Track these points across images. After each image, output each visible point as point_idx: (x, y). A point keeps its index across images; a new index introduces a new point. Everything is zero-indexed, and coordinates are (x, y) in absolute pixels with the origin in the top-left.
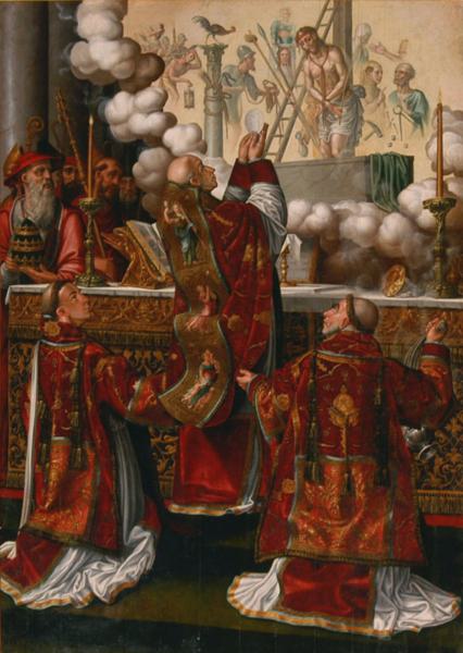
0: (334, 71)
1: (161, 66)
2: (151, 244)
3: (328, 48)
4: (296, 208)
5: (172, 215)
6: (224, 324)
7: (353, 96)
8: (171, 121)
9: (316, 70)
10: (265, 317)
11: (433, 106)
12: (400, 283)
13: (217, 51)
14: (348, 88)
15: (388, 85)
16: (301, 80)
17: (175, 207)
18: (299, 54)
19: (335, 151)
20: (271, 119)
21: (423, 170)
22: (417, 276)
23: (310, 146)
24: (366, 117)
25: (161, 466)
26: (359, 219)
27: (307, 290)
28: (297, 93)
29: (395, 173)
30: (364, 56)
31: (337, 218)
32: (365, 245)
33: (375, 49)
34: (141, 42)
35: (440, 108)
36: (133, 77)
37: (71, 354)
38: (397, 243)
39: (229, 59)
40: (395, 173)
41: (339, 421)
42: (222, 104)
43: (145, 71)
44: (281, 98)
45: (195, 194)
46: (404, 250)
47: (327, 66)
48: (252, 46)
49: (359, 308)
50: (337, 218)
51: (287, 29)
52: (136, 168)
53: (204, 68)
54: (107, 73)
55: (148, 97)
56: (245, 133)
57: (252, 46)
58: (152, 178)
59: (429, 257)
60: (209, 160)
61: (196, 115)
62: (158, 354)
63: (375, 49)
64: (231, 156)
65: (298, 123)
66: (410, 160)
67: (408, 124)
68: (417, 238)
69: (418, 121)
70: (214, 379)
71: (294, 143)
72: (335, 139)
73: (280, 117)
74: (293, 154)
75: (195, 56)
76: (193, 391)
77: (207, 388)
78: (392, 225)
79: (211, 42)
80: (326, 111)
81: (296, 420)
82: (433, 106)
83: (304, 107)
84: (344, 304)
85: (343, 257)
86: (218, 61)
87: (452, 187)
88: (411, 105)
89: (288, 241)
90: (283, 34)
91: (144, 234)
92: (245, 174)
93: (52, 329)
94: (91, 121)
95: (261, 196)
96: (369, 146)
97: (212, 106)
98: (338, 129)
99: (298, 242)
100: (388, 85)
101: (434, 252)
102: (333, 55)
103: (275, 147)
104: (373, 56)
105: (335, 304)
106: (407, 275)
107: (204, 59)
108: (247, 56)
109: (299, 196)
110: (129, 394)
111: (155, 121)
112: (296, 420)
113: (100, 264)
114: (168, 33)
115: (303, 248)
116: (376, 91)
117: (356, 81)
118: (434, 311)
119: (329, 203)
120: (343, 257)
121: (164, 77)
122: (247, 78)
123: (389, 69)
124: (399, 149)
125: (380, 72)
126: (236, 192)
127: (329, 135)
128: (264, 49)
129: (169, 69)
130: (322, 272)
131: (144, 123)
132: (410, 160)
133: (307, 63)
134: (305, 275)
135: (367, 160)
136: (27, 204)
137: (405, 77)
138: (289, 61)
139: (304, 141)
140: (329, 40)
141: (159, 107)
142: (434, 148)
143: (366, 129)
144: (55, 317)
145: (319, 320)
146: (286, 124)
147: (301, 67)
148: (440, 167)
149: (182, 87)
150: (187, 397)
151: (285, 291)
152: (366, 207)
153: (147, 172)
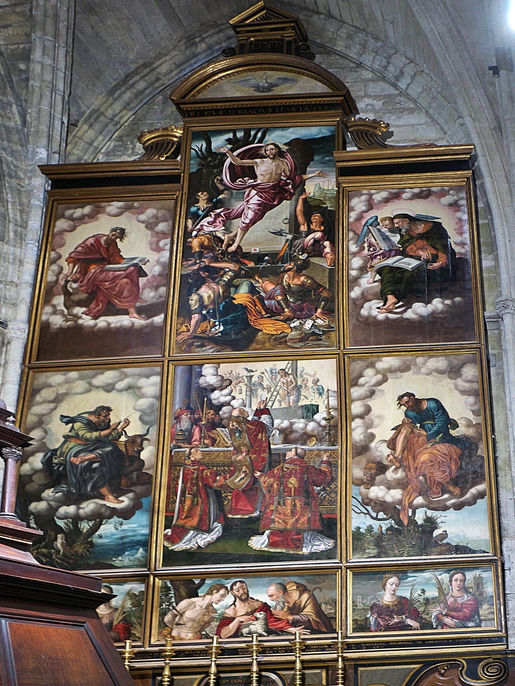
0: (291, 381)
1: (231, 382)
2: (225, 434)
3: (289, 374)
4: (277, 422)
5: (233, 426)
6: (250, 458)
7: (298, 388)
8: (234, 398)
9: (285, 381)
10: (266, 455)
11: (326, 390)
12: (314, 443)
13: (251, 377)
14: (296, 385)
15: (310, 384)
16: (279, 384)
17: (234, 424)
18: (279, 377)
19: (291, 404)
20: (269, 396)
21: (322, 408)
22: (320, 440)
23: (282, 403)
24: (302, 394)
25: (226, 503)
26: (299, 424)
27: (281, 446)
28: (278, 388)
29: (313, 410)
30: (302, 377)
31: (292, 424)
32: (302, 432)
33: (305, 374)
34: (224, 376)
35: (328, 390)
36: (221, 386)
37: (195, 469)
38: (313, 431)
39: (255, 379)
40: (313, 410)
41: (291, 486)
42: (252, 392)
43: (225, 384)
44: (272, 390)
45: (242, 419)
46: (315, 433)
47: (289, 380)
48: (263, 375)
49: (299, 451)
50: (292, 424)
51: (275, 370)
52: (221, 412)
53: (246, 382)
54: (212, 385)
55: (226, 391)
56: (259, 400)
57: (263, 375)
58: (226, 415)
59: (324, 434)
60: (246, 409)
61: (243, 396)
62: (226, 468)
63: (305, 374)
64: (254, 408)
65: (278, 397)
66: (318, 405)
67: (317, 395)
68: (320, 429)
69: (320, 394)
70: (246, 476)
71: (276, 402)
72: (291, 401)
73: (272, 395)
74: (276, 405)
75: (243, 379)
76: (239, 479)
77: (244, 478)
78: (311, 426)
79: (249, 374)
80: (288, 393)
81: (275, 486)
82: (326, 390)
83: (280, 392)
84: (294, 450)
85: (293, 436)
86: (251, 380)
87: (332, 413)
88: (318, 390)
89: (274, 432)
90: (273, 371)
91: (222, 431)
92: (259, 413)
93: (188, 462)
94: (206, 399)
95: (265, 419)
96: (303, 402)
97: (248, 393)
98: (292, 398)
99: (278, 432)
100: (310, 384)
101: (326, 433)
102: (291, 376)
103: (270, 404)
104: (305, 376)
105: (290, 450)
106: (317, 440)
107: (246, 380)
108: (261, 378)
109: (278, 418)
110: (215, 481)
111: (229, 398)
112: (275, 486)
113: (206, 441)
114: (234, 373)
115: (279, 434)
116: (306, 386)
117: (299, 384)
118: (326, 451)
119: (289, 420)
120: (293, 436)
121: (232, 385)
122: (261, 385)
123: (311, 380)
124: (314, 403)
125: (307, 381)
126: (256, 418)
127: (289, 400)
128: (267, 376)
129: (233, 383)
130: (286, 441)
131: (223, 399)
132: (318, 405)
133: (282, 379)
134: (280, 442)
135: (302, 406)
136: (182, 425)
137: (316, 382)
138: (275, 379)
139: (280, 402)
140: (290, 372)
141: (230, 394)
142: (326, 402)
143: (302, 397)
144: (189, 458)
145: (285, 455)
146: (274, 397)
147: (280, 380)
148: (328, 407)
149: (238, 388)
150: (236, 481)
151: (272, 447)
152: (302, 420)
153: (225, 413)
